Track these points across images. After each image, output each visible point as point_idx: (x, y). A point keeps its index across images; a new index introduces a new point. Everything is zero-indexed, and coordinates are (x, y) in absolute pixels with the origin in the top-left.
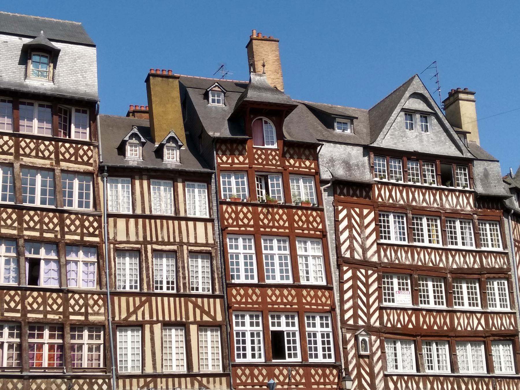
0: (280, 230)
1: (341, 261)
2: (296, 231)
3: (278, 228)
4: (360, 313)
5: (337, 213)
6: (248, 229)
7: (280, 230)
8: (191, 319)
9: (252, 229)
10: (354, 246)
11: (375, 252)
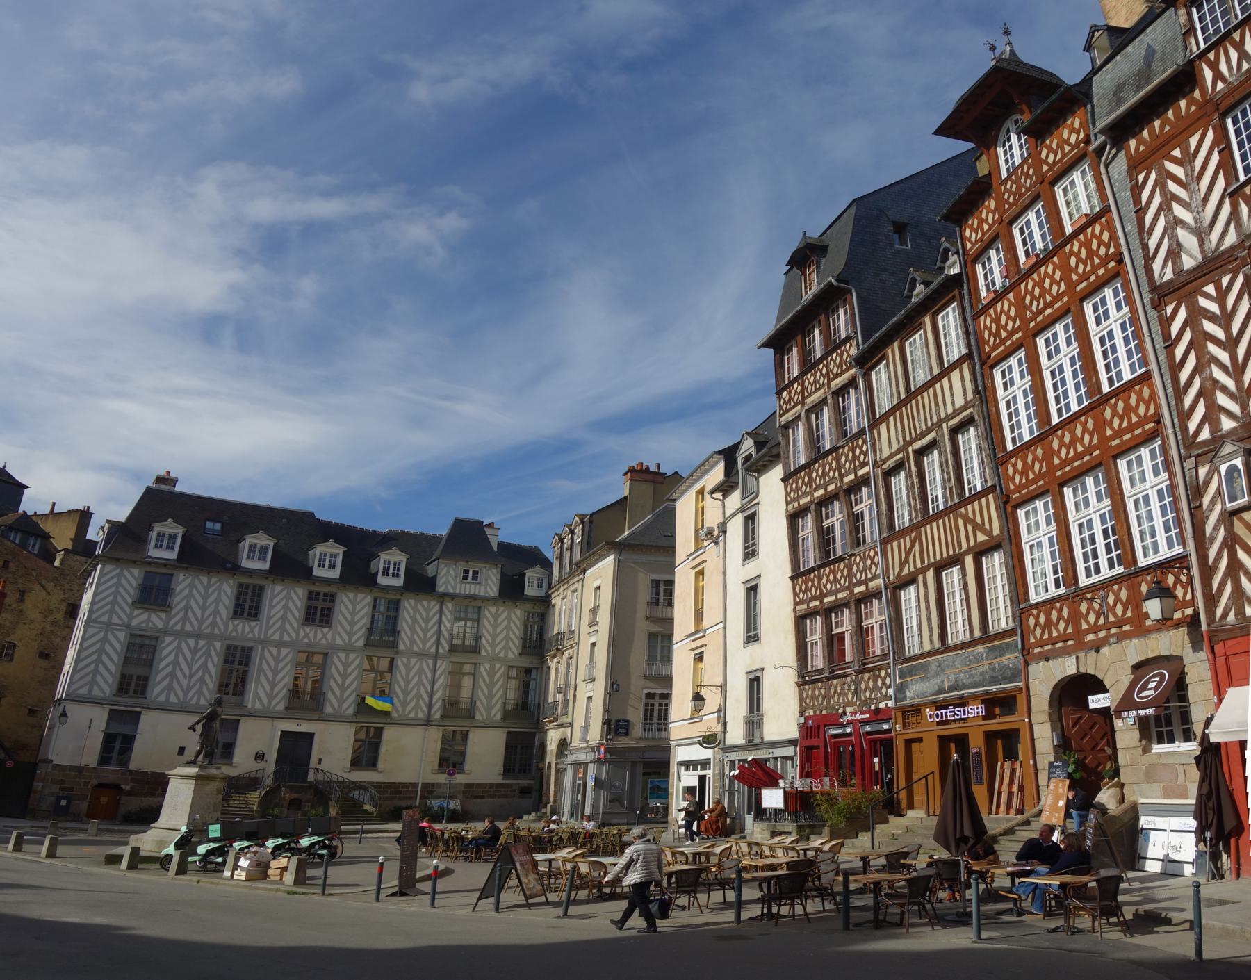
0: (1056, 306)
1: (1161, 294)
2: (1078, 288)
3: (1050, 305)
4: (1222, 400)
5: (1137, 190)
6: (1015, 338)
7: (1056, 306)
8: (965, 547)
9: (1020, 334)
10: (1179, 244)
11: (1228, 224)
